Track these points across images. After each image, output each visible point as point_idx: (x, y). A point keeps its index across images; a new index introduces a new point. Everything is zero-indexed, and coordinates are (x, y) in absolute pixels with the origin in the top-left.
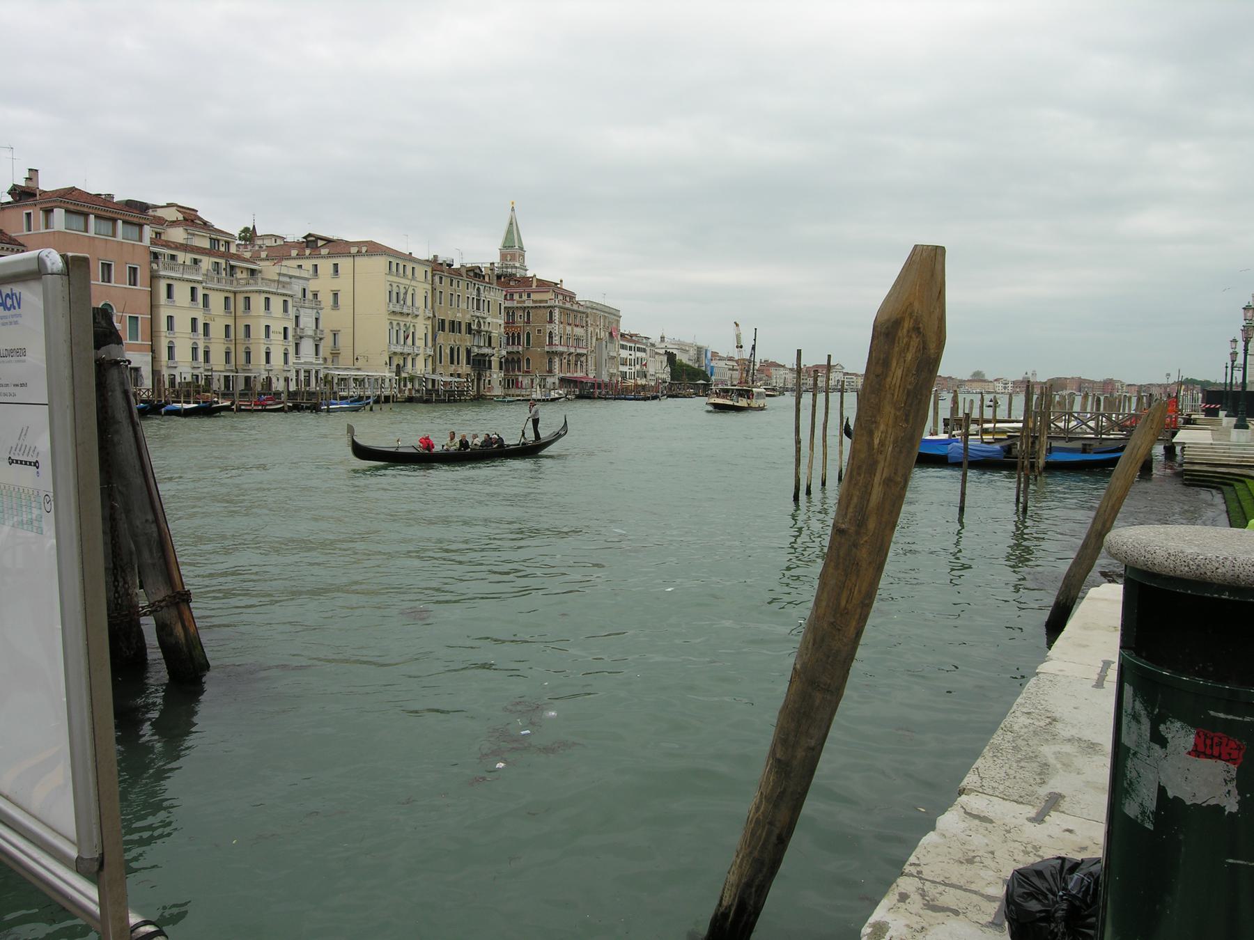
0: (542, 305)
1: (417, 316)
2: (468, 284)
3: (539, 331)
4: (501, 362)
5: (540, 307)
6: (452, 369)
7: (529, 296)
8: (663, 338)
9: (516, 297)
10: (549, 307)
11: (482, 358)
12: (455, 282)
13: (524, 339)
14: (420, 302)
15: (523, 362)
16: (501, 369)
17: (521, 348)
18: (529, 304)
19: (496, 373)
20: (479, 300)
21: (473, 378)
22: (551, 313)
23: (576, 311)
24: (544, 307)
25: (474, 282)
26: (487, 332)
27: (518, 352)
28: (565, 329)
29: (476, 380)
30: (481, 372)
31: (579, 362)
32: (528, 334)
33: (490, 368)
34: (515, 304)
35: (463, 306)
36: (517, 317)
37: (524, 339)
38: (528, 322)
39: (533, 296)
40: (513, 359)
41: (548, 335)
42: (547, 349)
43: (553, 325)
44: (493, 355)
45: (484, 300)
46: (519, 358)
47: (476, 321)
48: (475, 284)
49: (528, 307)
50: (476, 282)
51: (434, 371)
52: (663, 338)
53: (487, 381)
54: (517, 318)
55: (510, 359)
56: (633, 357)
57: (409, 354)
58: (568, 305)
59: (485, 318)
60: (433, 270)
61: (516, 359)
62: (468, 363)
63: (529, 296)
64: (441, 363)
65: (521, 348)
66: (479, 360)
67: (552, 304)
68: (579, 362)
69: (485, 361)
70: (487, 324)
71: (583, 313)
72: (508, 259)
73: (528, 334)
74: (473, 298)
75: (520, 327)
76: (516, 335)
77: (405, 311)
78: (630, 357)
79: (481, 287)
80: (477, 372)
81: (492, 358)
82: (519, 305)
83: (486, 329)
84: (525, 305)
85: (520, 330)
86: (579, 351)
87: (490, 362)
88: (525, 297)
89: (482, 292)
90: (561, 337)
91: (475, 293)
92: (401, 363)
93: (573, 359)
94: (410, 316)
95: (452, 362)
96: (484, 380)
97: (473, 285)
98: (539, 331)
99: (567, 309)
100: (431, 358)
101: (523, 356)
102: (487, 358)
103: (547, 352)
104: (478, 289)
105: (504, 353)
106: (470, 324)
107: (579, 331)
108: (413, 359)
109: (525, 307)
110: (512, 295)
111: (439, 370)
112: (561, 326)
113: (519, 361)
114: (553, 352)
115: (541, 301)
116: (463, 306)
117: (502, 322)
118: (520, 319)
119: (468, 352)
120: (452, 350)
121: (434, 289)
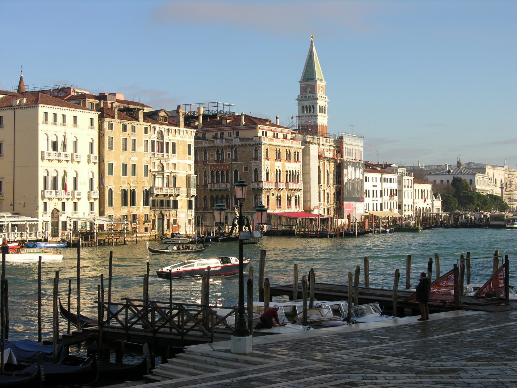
0: (248, 143)
1: (79, 162)
2: (146, 129)
3: (246, 168)
4: (190, 203)
5: (246, 145)
6: (125, 211)
7: (237, 134)
8: (459, 163)
9: (226, 134)
10: (254, 145)
11: (165, 199)
12: (129, 127)
13: (232, 177)
14: (83, 150)
15: (232, 199)
16: (190, 207)
17: (229, 186)
18: (236, 142)
19: (183, 212)
20: (162, 143)
21: (153, 218)
22: (256, 150)
23: (289, 147)
24: (250, 145)
25: (153, 125)
26: (171, 173)
27: (226, 190)
28: (273, 165)
29: (156, 220)
30: (163, 212)
31: (293, 199)
32: (236, 172)
33: (175, 206)
34: (223, 143)
35: (140, 148)
36: (226, 156)
37: (232, 177)
38: (236, 160)
39: (243, 134)
40: (222, 196)
41: (253, 172)
42: (253, 185)
43: (258, 162)
44: (178, 195)
45: (167, 143)
46: (228, 196)
47: (157, 163)
48: (155, 128)
49: (235, 145)
50: (157, 126)
51: (101, 213)
52: (459, 163)
53: (171, 221)
54: (226, 156)
55: (220, 196)
56: (379, 189)
57: (68, 199)
58: (276, 142)
59: (169, 159)
60: (101, 117)
61: (225, 196)
62: (146, 203)
63: (237, 134)
64: (111, 204)
65: (229, 186)
66: (162, 201)
67: (256, 142)
68: (293, 199)
69: (168, 201)
70: (171, 166)
71: (298, 148)
72: (308, 91)
73: (236, 172)
74: (153, 142)
75: (229, 164)
76: (225, 173)
77: (62, 158)
78: (375, 189)
79: (163, 130)
80: (158, 212)
81: (178, 198)
82: (228, 144)
83: (172, 169)
84: (233, 144)
85: (229, 168)
86: (292, 186)
87: (175, 202)
88: (234, 135)
89: (165, 134)
90: (267, 174)
91: (154, 137)
92: (60, 208)
93: (284, 195)
94: (70, 162)
95: (125, 204)
96: (168, 220)
97: (152, 129)
98: (246, 168)
99: (275, 146)
100: (97, 201)
101: (231, 194)
102: (172, 198)
103: (253, 189)
104: (161, 134)
105: (193, 192)
106: (146, 167)
107: (296, 167)
108: (75, 204)
109: (233, 146)
110: (222, 134)
111: (109, 211)
112: (268, 162)
113: (227, 198)
114: (258, 189)
115: (248, 139)
116: (140, 148)
117: (192, 162)
118: (229, 157)
119: (147, 194)
120: (124, 193)
121: (101, 136)
